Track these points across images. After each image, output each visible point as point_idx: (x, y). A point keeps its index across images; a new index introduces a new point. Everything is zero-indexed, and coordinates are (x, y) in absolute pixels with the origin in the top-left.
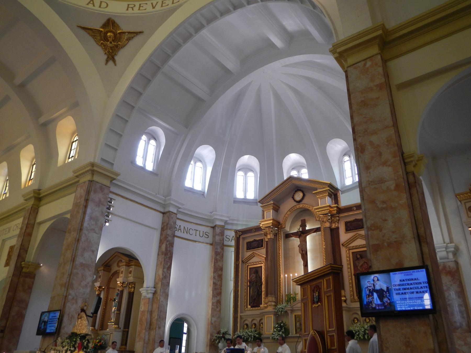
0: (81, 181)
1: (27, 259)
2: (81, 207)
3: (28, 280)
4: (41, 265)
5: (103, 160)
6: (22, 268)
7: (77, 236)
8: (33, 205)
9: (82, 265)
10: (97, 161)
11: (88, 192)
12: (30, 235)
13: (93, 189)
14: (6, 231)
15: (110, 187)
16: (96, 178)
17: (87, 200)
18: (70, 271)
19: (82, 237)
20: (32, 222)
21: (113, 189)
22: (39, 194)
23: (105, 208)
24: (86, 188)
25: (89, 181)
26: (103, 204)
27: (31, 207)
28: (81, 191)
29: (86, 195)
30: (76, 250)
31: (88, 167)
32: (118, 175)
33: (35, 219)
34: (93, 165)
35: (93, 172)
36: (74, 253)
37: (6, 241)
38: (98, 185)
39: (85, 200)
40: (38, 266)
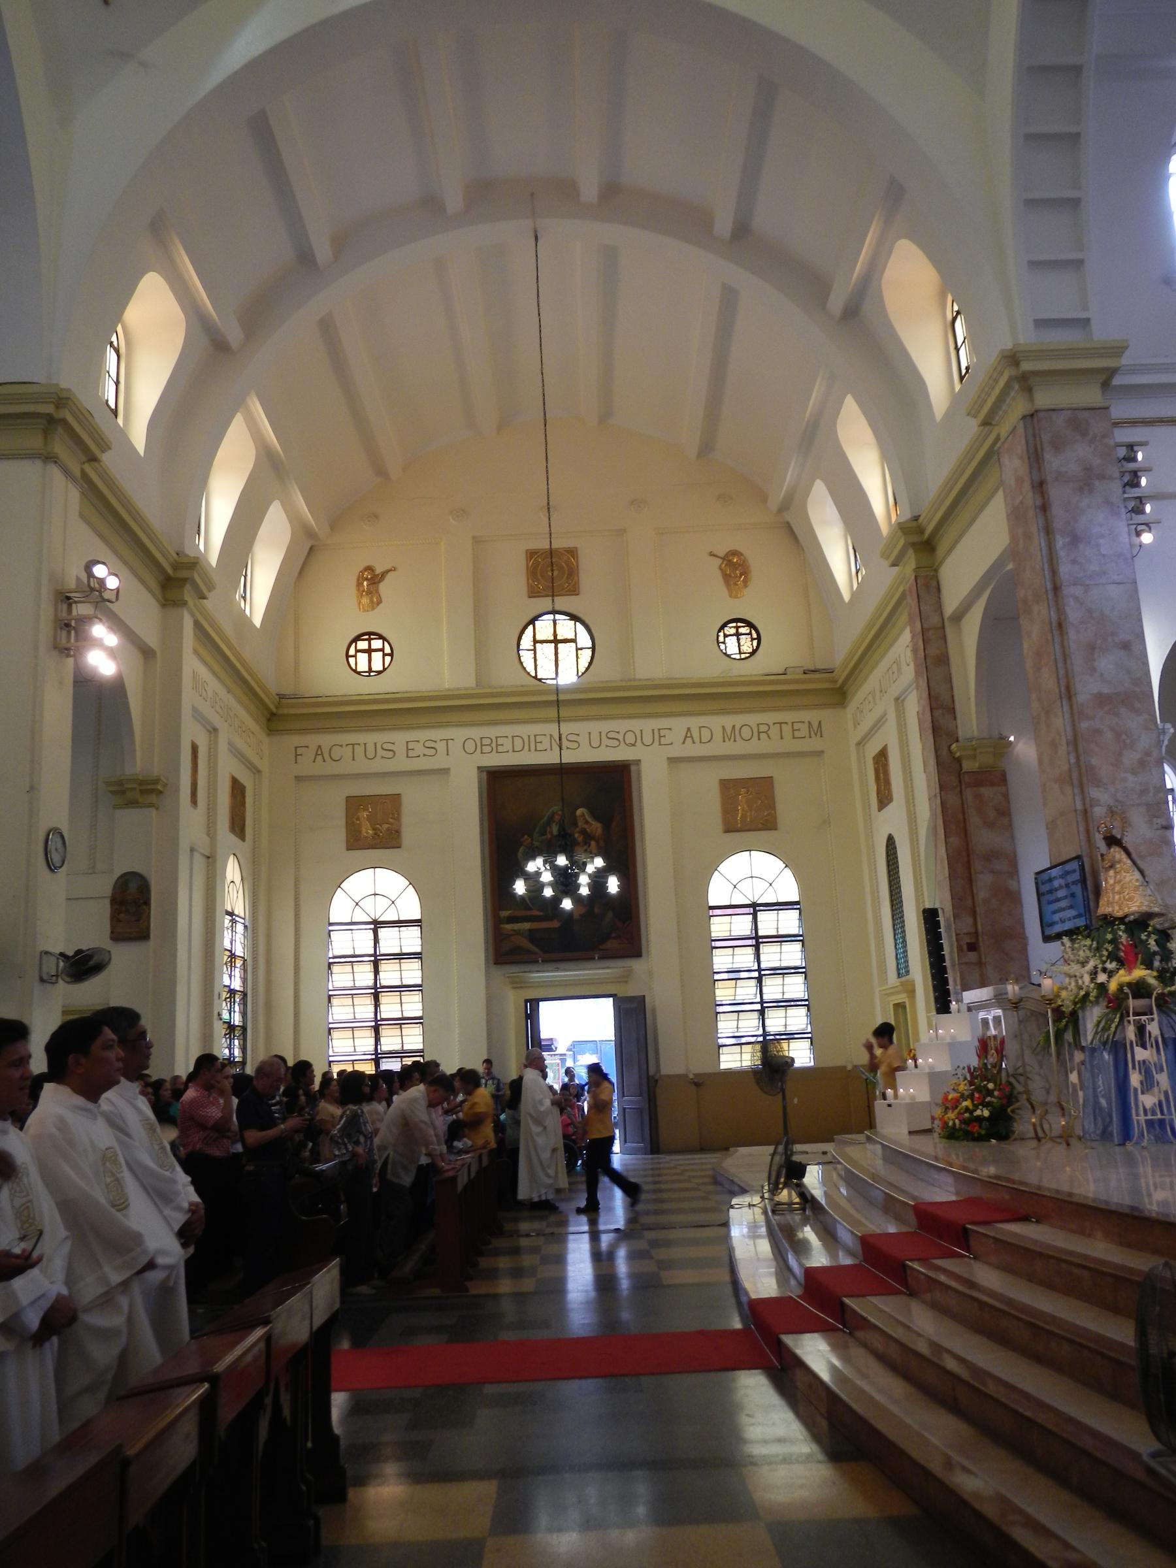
0: (1004, 430)
1: (961, 734)
2: (1031, 513)
3: (987, 792)
4: (1012, 739)
5: (1041, 324)
6: (959, 761)
7: (1052, 613)
8: (917, 569)
9: (1102, 700)
10: (1027, 337)
11: (1035, 457)
12: (943, 660)
13: (1046, 438)
14: (893, 673)
15: (1107, 408)
16: (1044, 398)
17: (1040, 486)
18: (1069, 729)
19: (1068, 610)
20: (935, 620)
21: (1120, 410)
22: (921, 531)
23: (1116, 487)
24: (1025, 447)
25: (1024, 417)
26: (1102, 477)
27: (913, 578)
28: (1013, 465)
29: (1031, 468)
30: (1065, 660)
31: (1001, 374)
32: (1118, 350)
33: (939, 607)
34: (1012, 358)
35: (1026, 382)
36: (1062, 672)
37: (903, 701)
38: (1060, 420)
39: (1033, 487)
40: (1001, 746)
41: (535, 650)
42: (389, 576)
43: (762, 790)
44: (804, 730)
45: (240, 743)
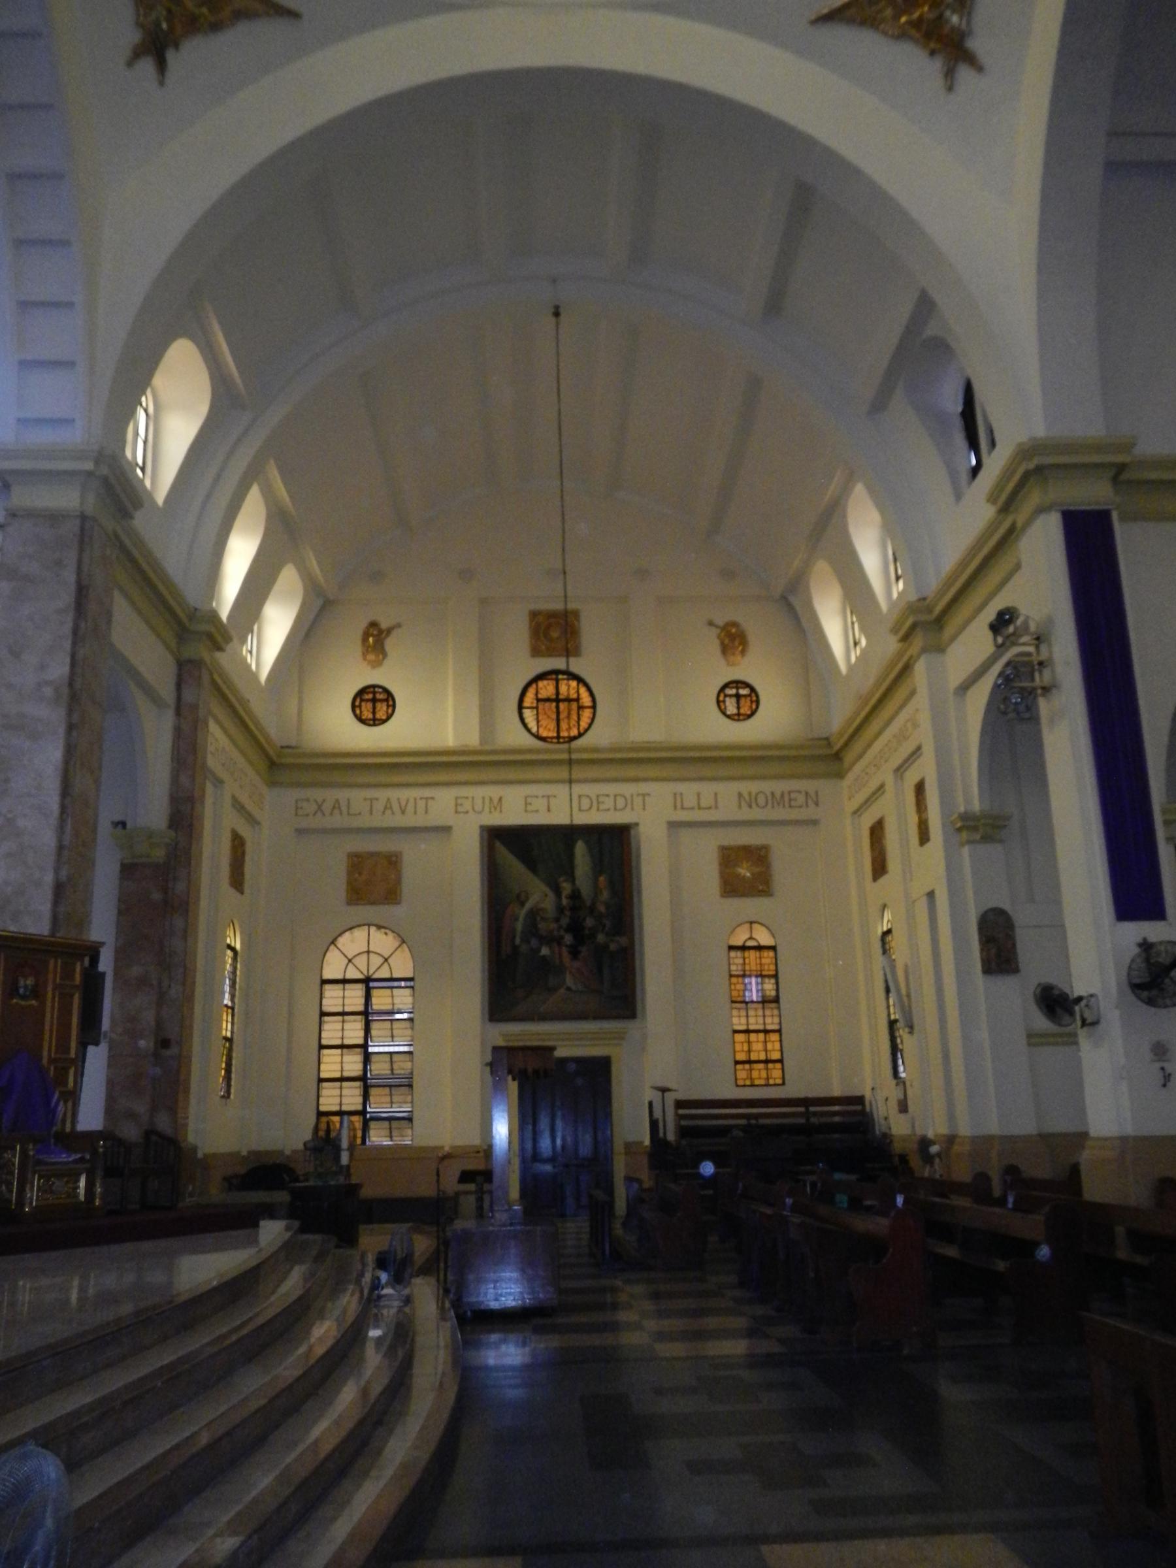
41: (537, 708)
42: (394, 633)
43: (759, 856)
44: (801, 799)
45: (244, 799)
